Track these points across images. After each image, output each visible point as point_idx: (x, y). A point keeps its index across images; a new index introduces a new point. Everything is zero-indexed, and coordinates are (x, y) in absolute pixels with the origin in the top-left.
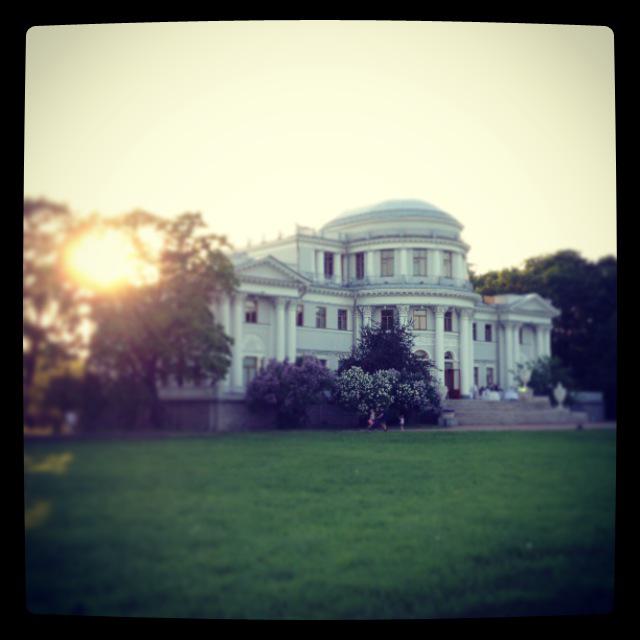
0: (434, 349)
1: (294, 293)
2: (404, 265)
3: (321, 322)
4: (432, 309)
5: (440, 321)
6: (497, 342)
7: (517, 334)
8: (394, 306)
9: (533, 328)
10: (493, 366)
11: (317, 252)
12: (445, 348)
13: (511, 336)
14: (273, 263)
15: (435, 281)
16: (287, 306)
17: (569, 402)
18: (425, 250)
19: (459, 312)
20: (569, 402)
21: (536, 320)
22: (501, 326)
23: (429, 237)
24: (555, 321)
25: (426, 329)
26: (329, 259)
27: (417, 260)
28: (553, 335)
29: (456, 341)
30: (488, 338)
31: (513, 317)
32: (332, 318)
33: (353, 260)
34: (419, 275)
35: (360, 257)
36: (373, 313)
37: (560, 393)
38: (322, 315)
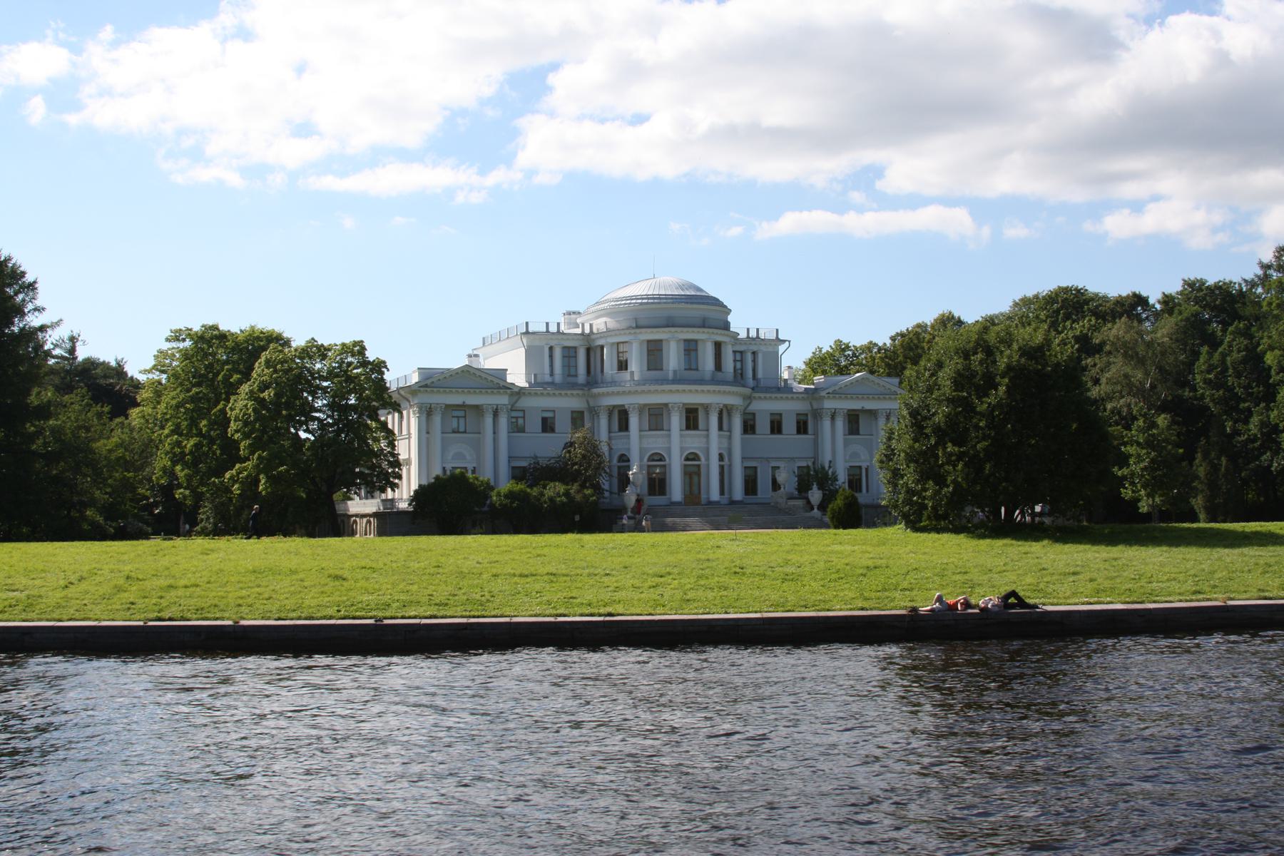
0: (669, 450)
1: (503, 400)
6: (816, 434)
7: (840, 424)
8: (623, 406)
11: (551, 349)
12: (682, 449)
14: (472, 371)
15: (671, 376)
16: (496, 414)
18: (661, 341)
19: (706, 408)
25: (663, 430)
29: (705, 440)
30: (802, 428)
31: (829, 404)
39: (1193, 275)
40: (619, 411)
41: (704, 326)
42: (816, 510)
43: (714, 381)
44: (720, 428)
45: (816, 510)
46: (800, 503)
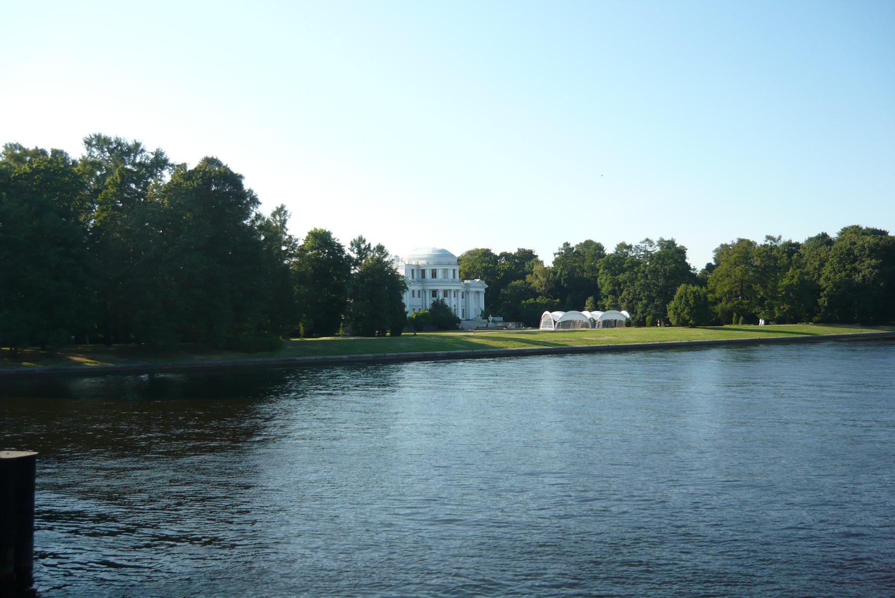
0: (450, 304)
2: (440, 275)
3: (413, 296)
4: (450, 290)
5: (453, 294)
9: (478, 292)
10: (464, 308)
13: (471, 296)
17: (493, 321)
18: (447, 269)
20: (493, 321)
21: (479, 290)
22: (467, 292)
23: (449, 264)
24: (486, 289)
26: (413, 270)
27: (444, 273)
28: (485, 294)
31: (472, 289)
32: (416, 293)
33: (421, 271)
34: (445, 278)
35: (423, 271)
36: (430, 292)
37: (491, 318)
38: (413, 291)
39: (522, 246)
40: (433, 291)
41: (449, 265)
42: (491, 323)
43: (453, 282)
44: (455, 296)
45: (491, 323)
46: (486, 320)
